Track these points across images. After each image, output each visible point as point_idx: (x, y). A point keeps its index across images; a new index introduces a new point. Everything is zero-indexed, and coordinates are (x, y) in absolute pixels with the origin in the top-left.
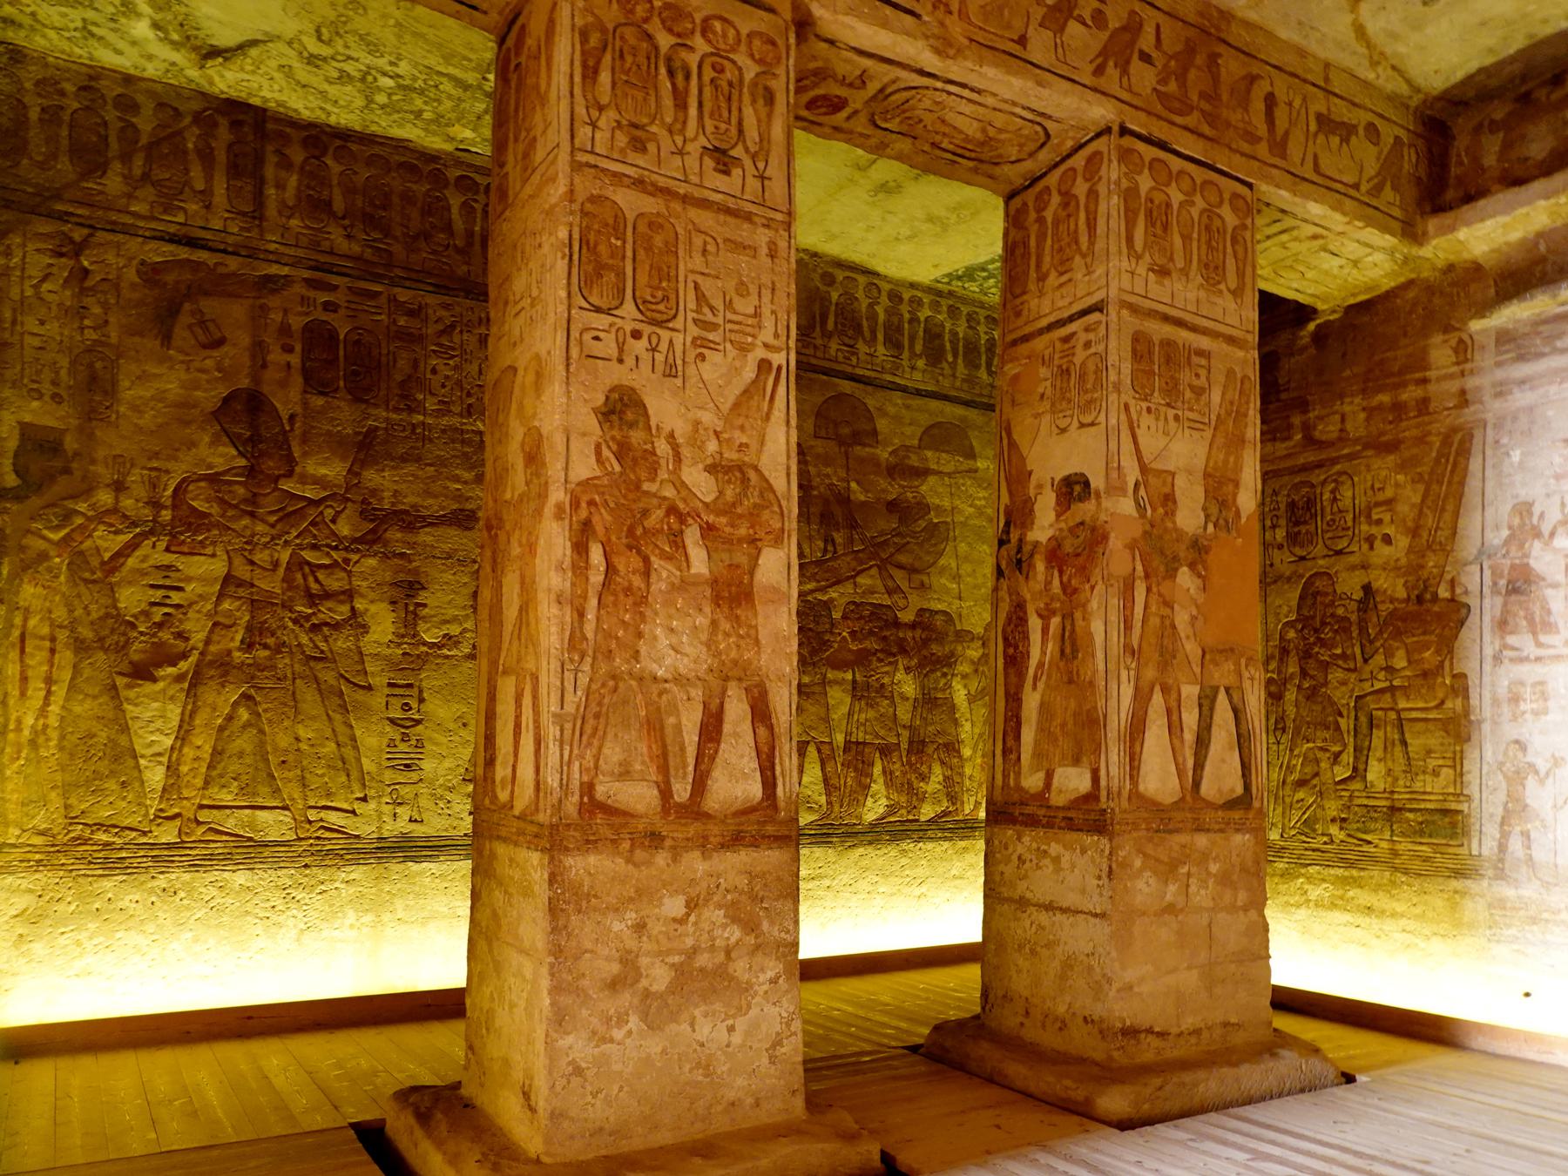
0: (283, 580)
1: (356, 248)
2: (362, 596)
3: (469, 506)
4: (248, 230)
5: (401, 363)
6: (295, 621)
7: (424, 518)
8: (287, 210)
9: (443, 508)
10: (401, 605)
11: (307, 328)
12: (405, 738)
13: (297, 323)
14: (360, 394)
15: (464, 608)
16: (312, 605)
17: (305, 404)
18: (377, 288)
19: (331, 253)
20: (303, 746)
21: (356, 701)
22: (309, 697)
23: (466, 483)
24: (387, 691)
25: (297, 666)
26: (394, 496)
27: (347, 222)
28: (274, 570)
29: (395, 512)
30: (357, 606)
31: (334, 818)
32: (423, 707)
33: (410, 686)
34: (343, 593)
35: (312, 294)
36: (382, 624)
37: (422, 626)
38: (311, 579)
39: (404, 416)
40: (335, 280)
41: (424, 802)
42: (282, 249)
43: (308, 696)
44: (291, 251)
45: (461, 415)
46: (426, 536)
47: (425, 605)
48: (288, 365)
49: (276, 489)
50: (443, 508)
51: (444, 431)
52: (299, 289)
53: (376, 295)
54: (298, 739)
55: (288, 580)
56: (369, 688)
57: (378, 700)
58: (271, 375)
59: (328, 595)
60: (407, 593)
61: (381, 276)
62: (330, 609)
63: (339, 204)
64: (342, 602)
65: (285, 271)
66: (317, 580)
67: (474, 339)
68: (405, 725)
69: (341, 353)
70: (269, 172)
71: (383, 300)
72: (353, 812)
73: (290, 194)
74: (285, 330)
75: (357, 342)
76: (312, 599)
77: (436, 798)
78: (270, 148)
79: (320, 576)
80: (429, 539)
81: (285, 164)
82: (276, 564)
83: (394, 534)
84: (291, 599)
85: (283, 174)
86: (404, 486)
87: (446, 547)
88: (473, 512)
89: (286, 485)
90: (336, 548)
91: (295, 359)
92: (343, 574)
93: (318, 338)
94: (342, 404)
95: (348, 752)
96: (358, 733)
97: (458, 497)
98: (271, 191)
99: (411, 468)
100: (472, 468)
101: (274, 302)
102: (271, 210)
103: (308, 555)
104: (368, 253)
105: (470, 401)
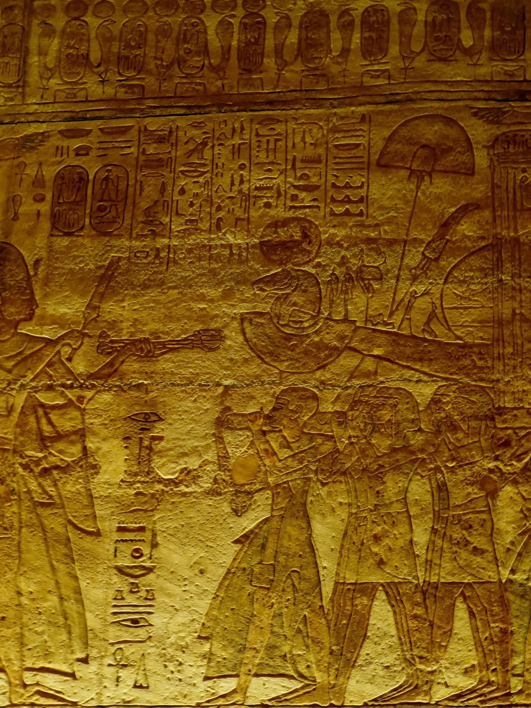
0: (17, 425)
1: (110, 91)
2: (94, 434)
3: (213, 325)
4: (12, 99)
5: (147, 190)
6: (25, 467)
7: (164, 344)
8: (48, 72)
9: (185, 331)
10: (134, 441)
11: (60, 176)
12: (134, 589)
13: (49, 173)
14: (102, 231)
15: (205, 437)
16: (44, 447)
17: (50, 248)
18: (129, 123)
19: (87, 101)
20: (24, 600)
21: (82, 549)
22: (33, 547)
23: (212, 301)
24: (116, 536)
25: (25, 516)
26: (134, 325)
27: (102, 69)
28: (7, 416)
29: (133, 343)
30: (89, 445)
31: (51, 682)
32: (156, 553)
33: (142, 529)
34: (75, 433)
35: (65, 143)
36: (114, 461)
37: (157, 462)
38: (44, 421)
39: (148, 241)
40: (88, 125)
41: (152, 664)
42: (41, 108)
43: (33, 546)
44: (50, 109)
45: (210, 231)
46: (165, 364)
47: (161, 438)
48: (39, 213)
49: (16, 334)
50: (185, 331)
51: (190, 251)
52: (55, 141)
53: (128, 129)
54: (19, 593)
55: (21, 425)
56: (98, 534)
57: (106, 547)
58: (23, 225)
59: (59, 437)
60: (143, 426)
61: (132, 110)
62: (60, 452)
63: (95, 56)
64: (73, 443)
65: (44, 127)
66: (50, 422)
67: (225, 152)
68: (133, 574)
69: (90, 192)
70: (34, 43)
71: (133, 134)
72: (73, 675)
73: (51, 60)
74: (38, 182)
75: (106, 179)
76: (43, 441)
77: (166, 659)
78: (35, 22)
79: (53, 417)
80: (169, 366)
81: (49, 31)
82: (10, 410)
83: (131, 366)
84: (23, 444)
85: (45, 41)
86: (144, 314)
87: (186, 372)
88: (219, 331)
89: (25, 329)
90: (71, 387)
91: (45, 207)
92: (77, 413)
93: (72, 182)
94: (86, 241)
95: (71, 606)
96: (83, 584)
97: (203, 317)
98: (34, 59)
99: (153, 293)
100: (220, 283)
101: (30, 158)
102: (33, 77)
103: (43, 397)
104: (121, 94)
105: (221, 214)
